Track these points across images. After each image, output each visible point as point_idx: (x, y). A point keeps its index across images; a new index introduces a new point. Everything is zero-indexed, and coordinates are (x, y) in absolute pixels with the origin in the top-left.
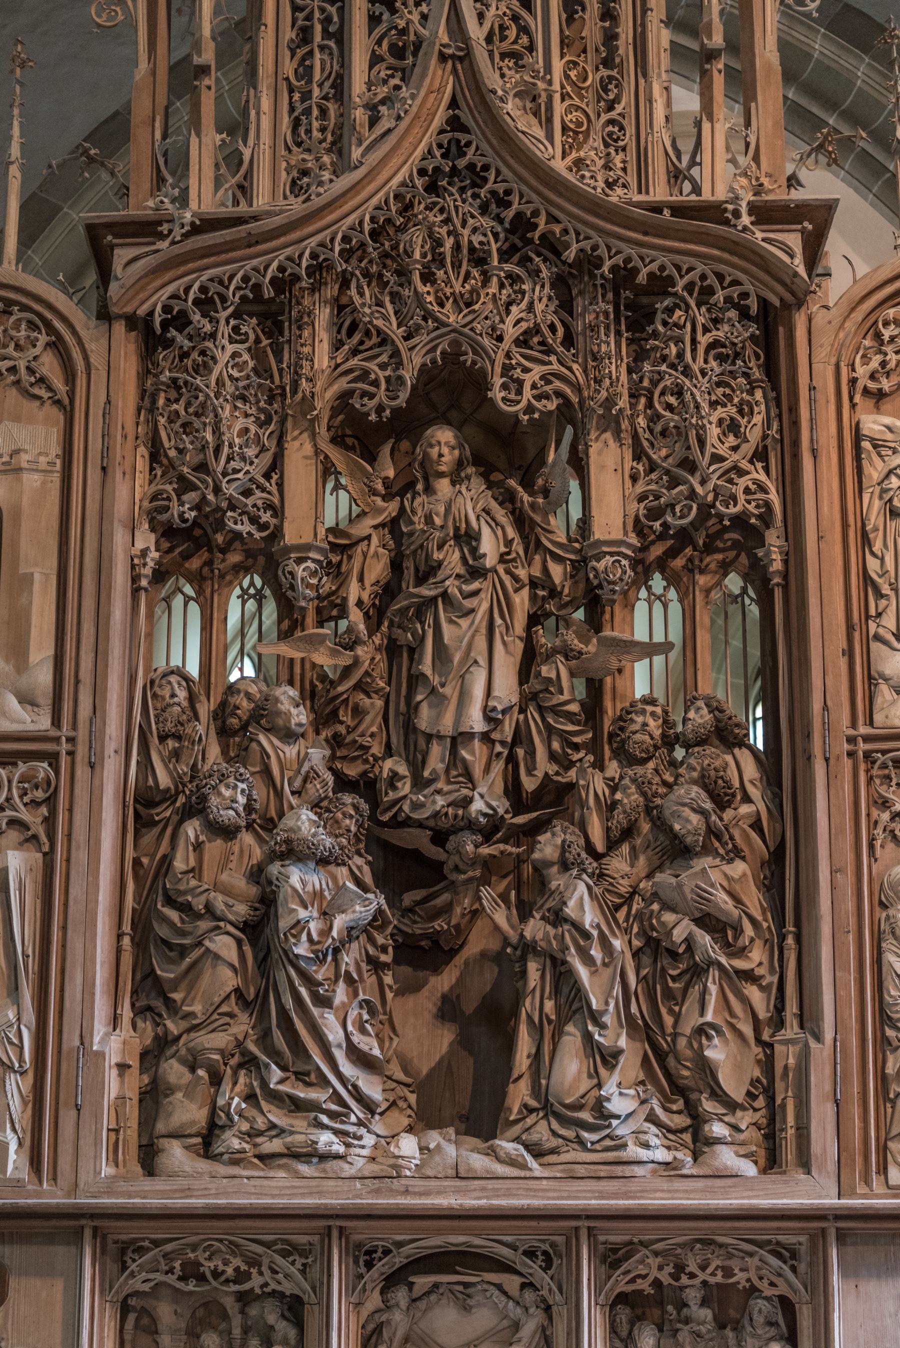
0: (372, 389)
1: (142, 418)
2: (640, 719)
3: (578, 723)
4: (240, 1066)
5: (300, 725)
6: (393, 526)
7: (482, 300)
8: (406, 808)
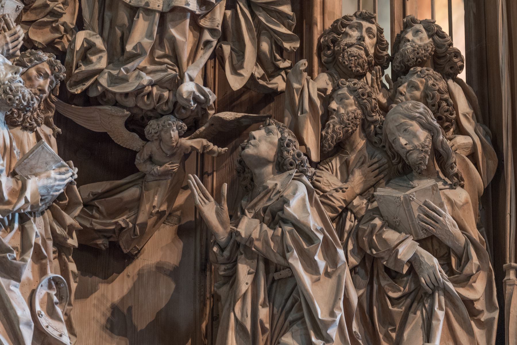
2: (355, 34)
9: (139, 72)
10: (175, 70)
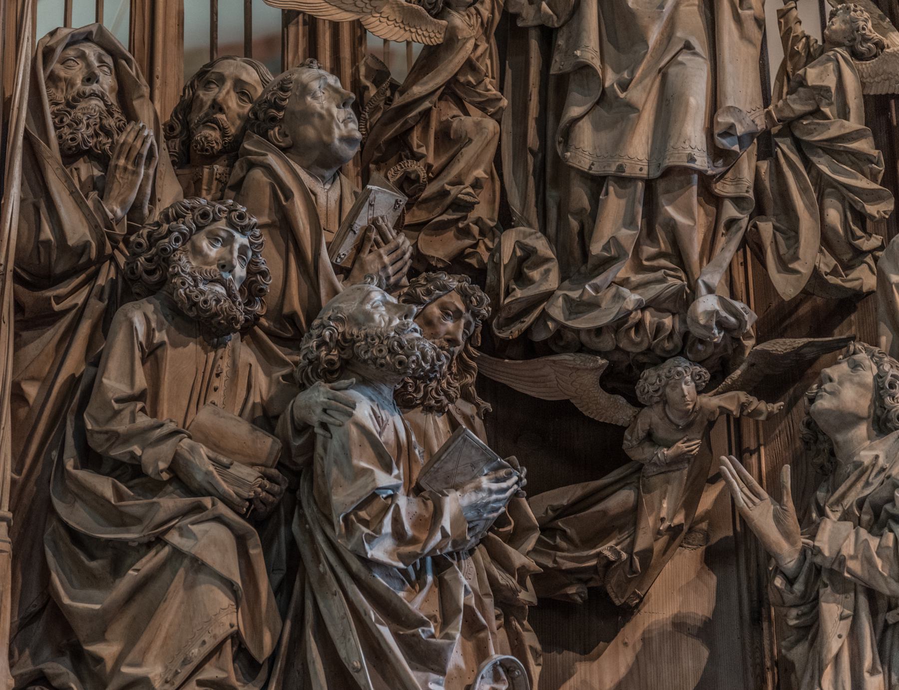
9: (618, 289)
10: (680, 278)
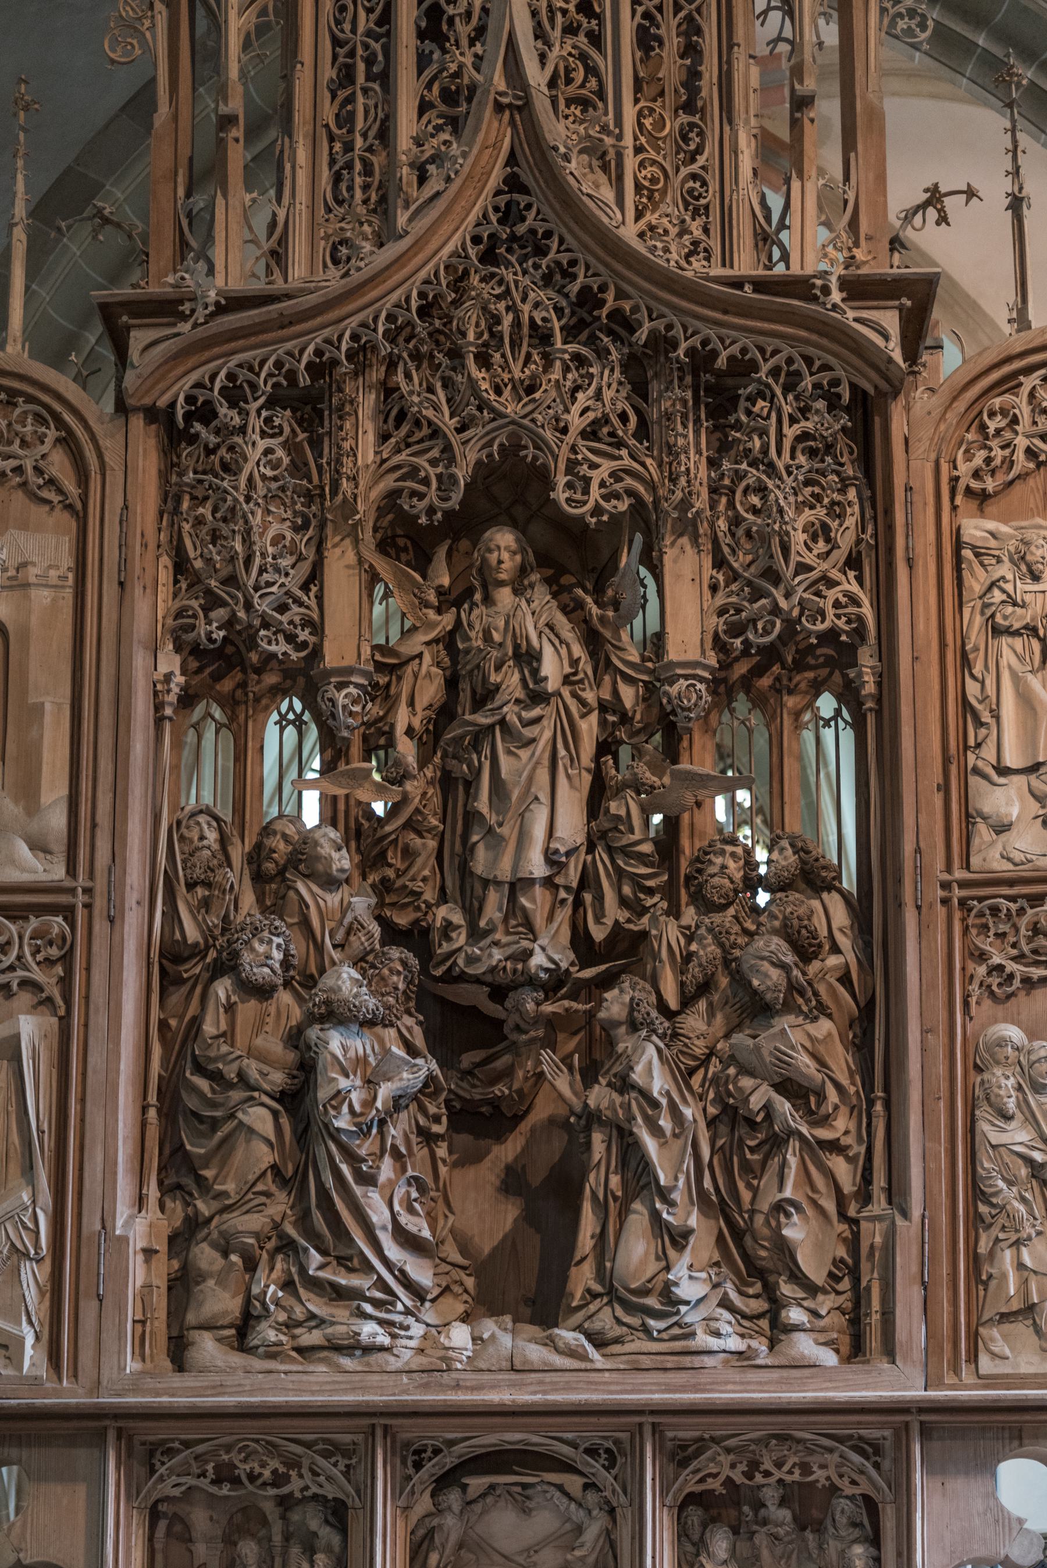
0: (422, 488)
1: (164, 523)
2: (719, 860)
3: (651, 865)
4: (278, 1250)
5: (342, 870)
6: (449, 641)
7: (544, 387)
8: (461, 962)
